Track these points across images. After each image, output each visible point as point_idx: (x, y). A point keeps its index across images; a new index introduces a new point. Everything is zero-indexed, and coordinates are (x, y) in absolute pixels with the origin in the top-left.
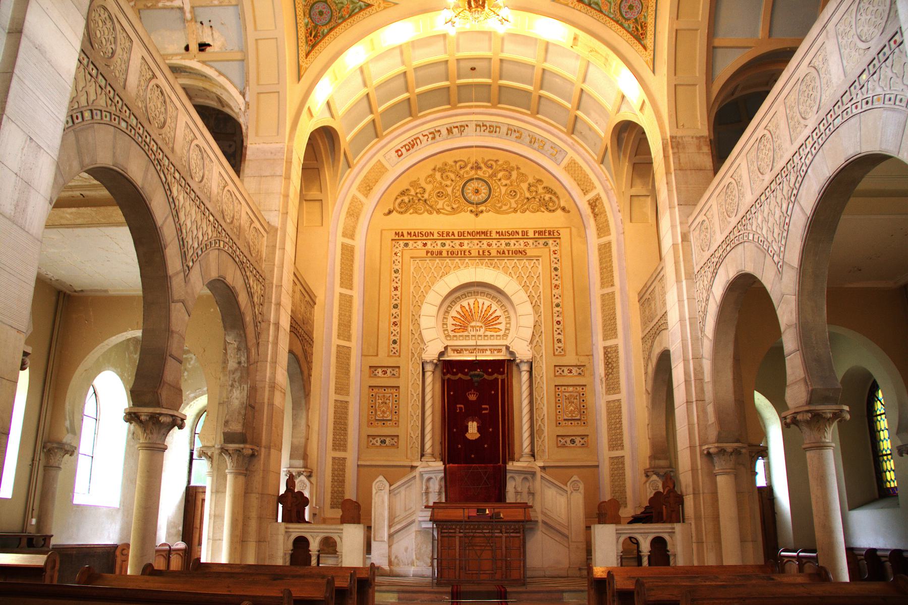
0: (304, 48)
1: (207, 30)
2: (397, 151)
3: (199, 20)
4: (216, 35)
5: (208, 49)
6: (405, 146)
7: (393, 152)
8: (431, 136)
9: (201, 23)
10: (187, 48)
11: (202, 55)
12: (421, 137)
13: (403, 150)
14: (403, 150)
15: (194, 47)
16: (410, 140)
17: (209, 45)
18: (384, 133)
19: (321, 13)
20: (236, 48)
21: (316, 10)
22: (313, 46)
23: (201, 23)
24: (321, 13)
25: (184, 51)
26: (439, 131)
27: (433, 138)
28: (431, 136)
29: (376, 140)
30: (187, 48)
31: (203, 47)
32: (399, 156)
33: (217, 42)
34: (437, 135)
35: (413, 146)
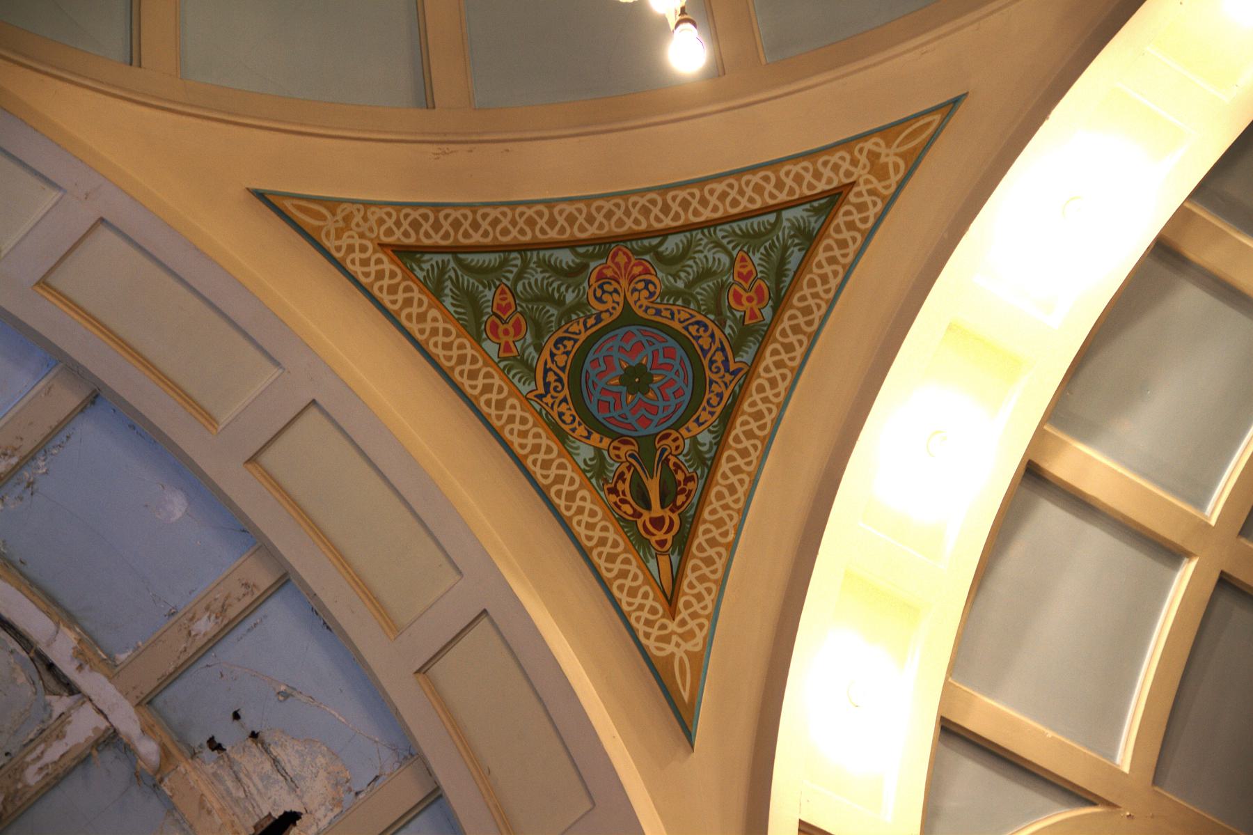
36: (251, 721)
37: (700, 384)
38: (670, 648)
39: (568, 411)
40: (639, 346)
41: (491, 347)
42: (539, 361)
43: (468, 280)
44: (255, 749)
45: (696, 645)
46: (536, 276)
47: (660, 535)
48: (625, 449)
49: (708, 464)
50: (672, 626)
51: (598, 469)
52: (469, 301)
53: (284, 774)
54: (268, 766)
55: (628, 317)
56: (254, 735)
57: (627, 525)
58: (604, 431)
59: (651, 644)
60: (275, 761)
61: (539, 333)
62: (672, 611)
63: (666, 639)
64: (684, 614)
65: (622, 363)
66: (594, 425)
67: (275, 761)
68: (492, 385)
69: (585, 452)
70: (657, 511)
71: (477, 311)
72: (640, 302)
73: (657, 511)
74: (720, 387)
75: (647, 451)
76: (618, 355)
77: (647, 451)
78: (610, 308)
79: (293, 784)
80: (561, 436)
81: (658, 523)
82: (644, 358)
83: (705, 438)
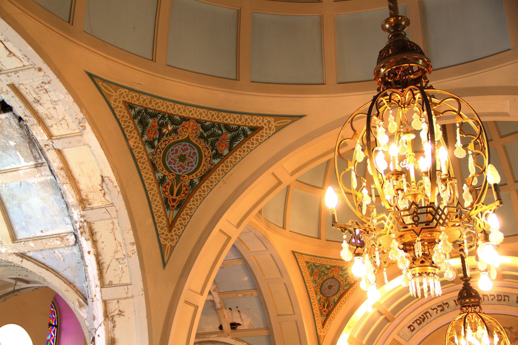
0: (320, 320)
1: (236, 314)
2: (409, 327)
3: (228, 307)
4: (244, 317)
5: (239, 328)
6: (416, 321)
7: (406, 328)
8: (439, 309)
9: (230, 309)
10: (221, 327)
11: (235, 334)
12: (431, 311)
13: (415, 325)
14: (415, 325)
15: (227, 327)
16: (420, 316)
17: (239, 324)
18: (395, 316)
19: (330, 287)
20: (262, 326)
21: (326, 286)
22: (328, 315)
23: (230, 309)
24: (330, 287)
25: (218, 330)
26: (447, 303)
27: (441, 311)
28: (439, 309)
29: (389, 324)
30: (221, 327)
31: (234, 326)
32: (412, 331)
33: (245, 322)
34: (445, 307)
35: (424, 320)
36: (239, 309)
37: (339, 290)
38: (321, 334)
39: (319, 290)
40: (332, 282)
41: (312, 278)
42: (318, 281)
43: (314, 267)
44: (238, 313)
45: (324, 334)
46: (323, 268)
47: (324, 313)
48: (324, 298)
49: (336, 304)
50: (322, 330)
51: (319, 301)
52: (313, 270)
53: (241, 318)
54: (239, 316)
55: (333, 277)
56: (239, 311)
57: (321, 310)
58: (322, 294)
59: (318, 332)
60: (240, 316)
61: (320, 277)
62: (323, 328)
63: (321, 332)
64: (324, 328)
65: (329, 284)
66: (321, 293)
67: (240, 316)
68: (311, 286)
69: (319, 297)
70: (325, 309)
71: (313, 272)
72: (336, 275)
73: (325, 309)
74: (341, 291)
75: (327, 299)
76: (329, 283)
77: (327, 299)
78: (331, 275)
79: (242, 320)
80: (316, 294)
81: (325, 311)
82: (332, 284)
83: (336, 299)
